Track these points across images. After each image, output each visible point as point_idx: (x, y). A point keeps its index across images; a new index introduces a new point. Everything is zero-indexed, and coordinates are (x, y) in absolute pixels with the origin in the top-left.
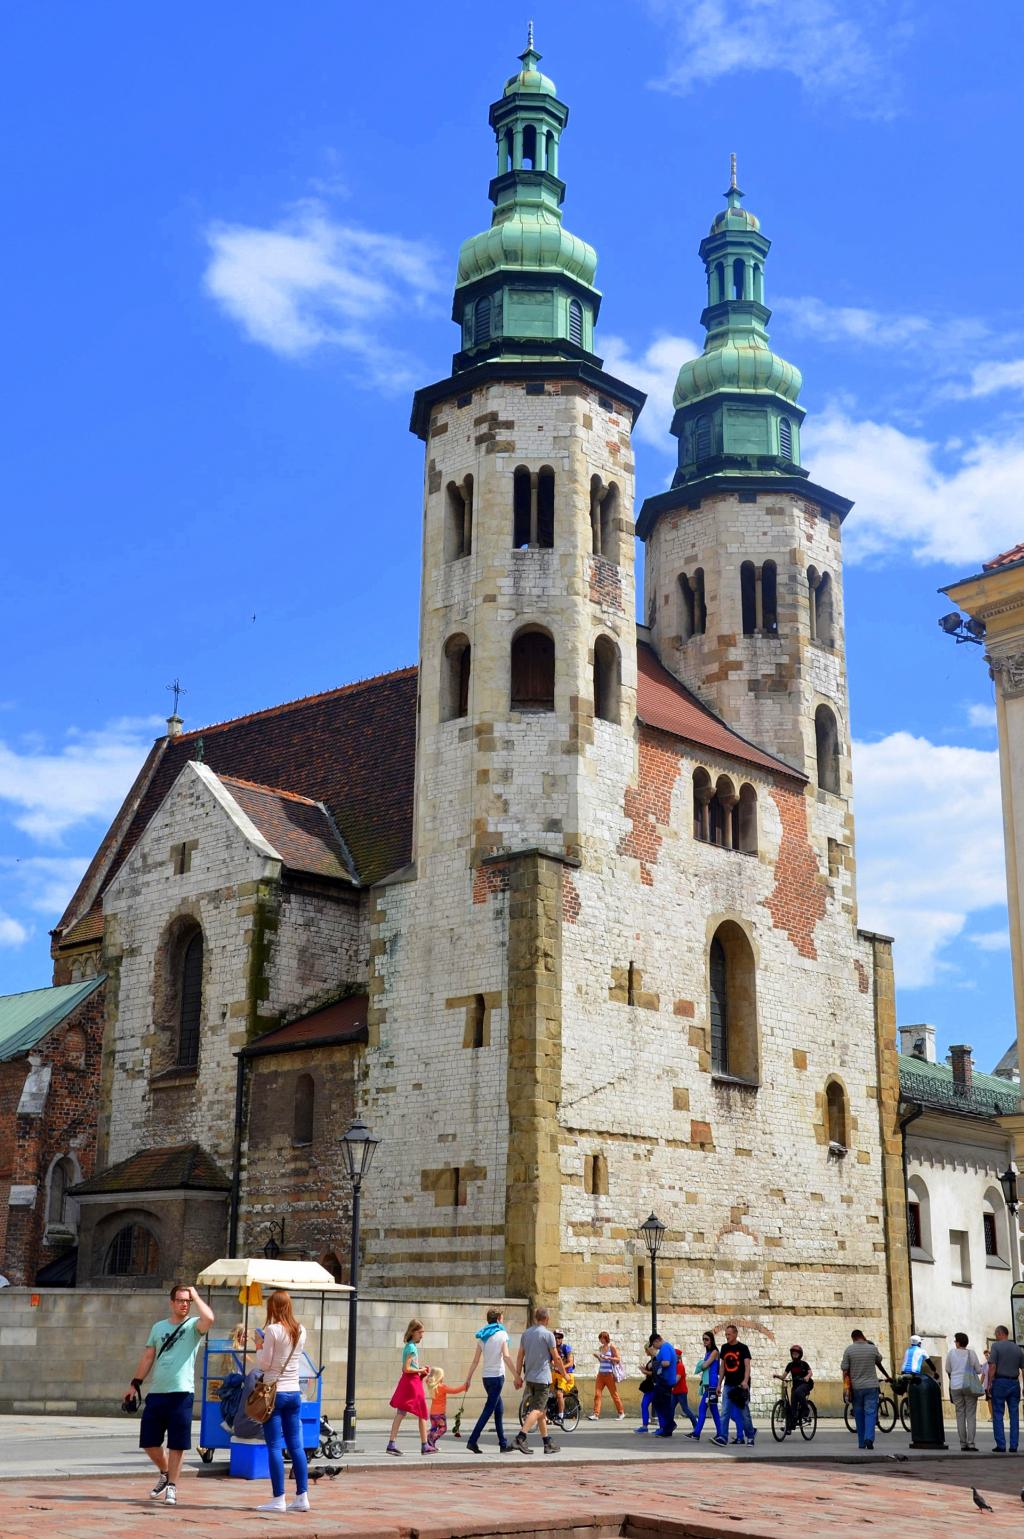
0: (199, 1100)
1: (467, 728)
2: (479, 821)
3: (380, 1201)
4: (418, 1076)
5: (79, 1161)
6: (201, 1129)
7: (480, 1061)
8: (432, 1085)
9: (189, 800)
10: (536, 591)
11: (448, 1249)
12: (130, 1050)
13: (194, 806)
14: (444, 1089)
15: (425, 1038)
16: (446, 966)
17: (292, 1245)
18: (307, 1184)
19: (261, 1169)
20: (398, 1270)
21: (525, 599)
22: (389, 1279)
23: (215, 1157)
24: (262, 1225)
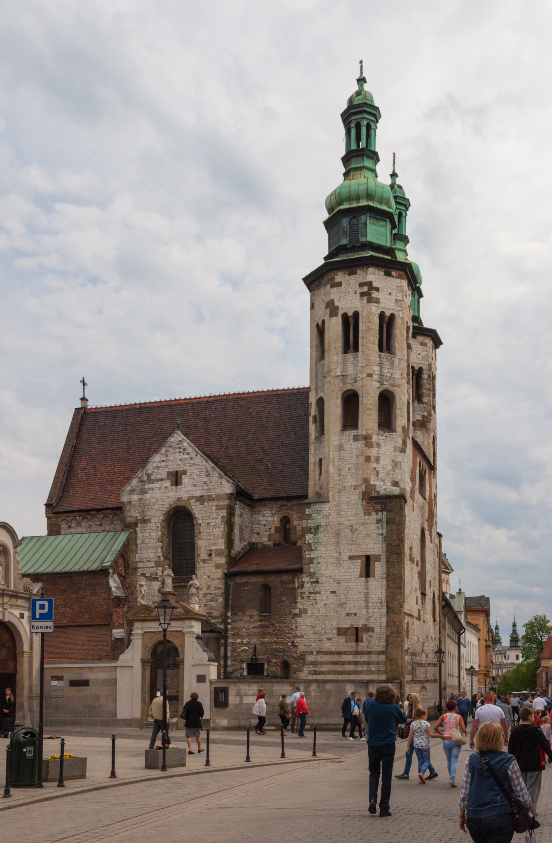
4: (334, 588)
7: (369, 583)
8: (343, 592)
9: (178, 450)
11: (353, 660)
12: (148, 568)
13: (182, 454)
16: (348, 542)
17: (262, 657)
19: (239, 625)
20: (325, 668)
22: (320, 671)
23: (210, 618)
24: (242, 648)
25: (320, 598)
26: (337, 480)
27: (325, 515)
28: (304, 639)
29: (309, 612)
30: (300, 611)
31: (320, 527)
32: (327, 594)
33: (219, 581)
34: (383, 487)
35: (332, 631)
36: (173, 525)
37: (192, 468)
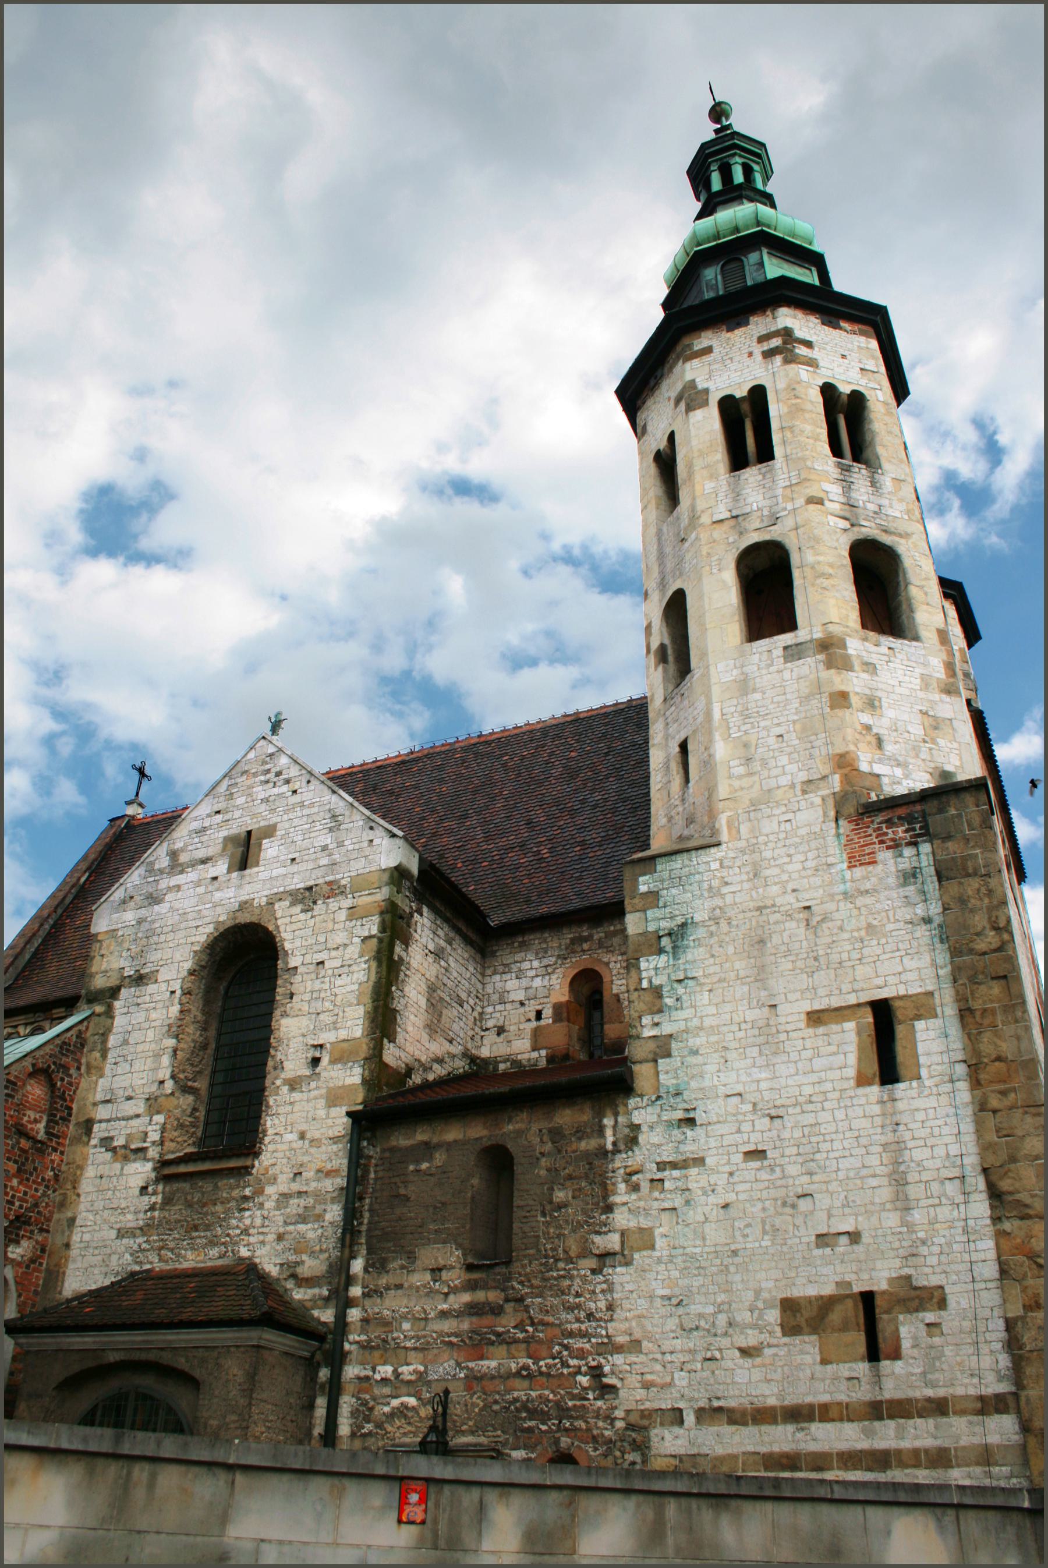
0: (260, 1192)
1: (797, 645)
2: (842, 756)
3: (681, 1357)
5: (16, 1282)
6: (261, 1238)
7: (900, 1105)
8: (794, 1150)
9: (262, 778)
10: (871, 507)
12: (123, 1119)
14: (818, 1156)
15: (763, 1075)
18: (500, 1329)
19: (391, 1304)
21: (860, 511)
23: (290, 1284)
24: (395, 1403)
25: (703, 1183)
26: (740, 777)
27: (705, 885)
28: (642, 1358)
29: (659, 1243)
30: (623, 1243)
31: (690, 930)
32: (729, 1163)
33: (335, 1147)
34: (905, 782)
35: (760, 1317)
36: (226, 993)
37: (291, 816)
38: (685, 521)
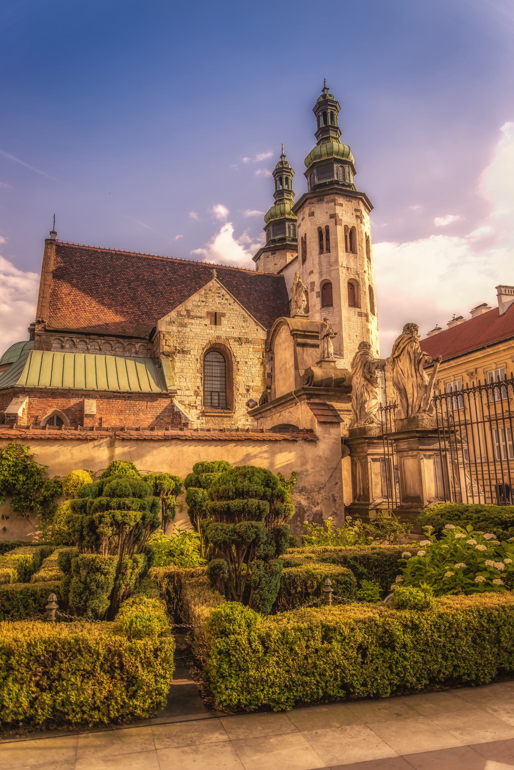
12: (186, 396)
26: (348, 343)
38: (332, 259)
